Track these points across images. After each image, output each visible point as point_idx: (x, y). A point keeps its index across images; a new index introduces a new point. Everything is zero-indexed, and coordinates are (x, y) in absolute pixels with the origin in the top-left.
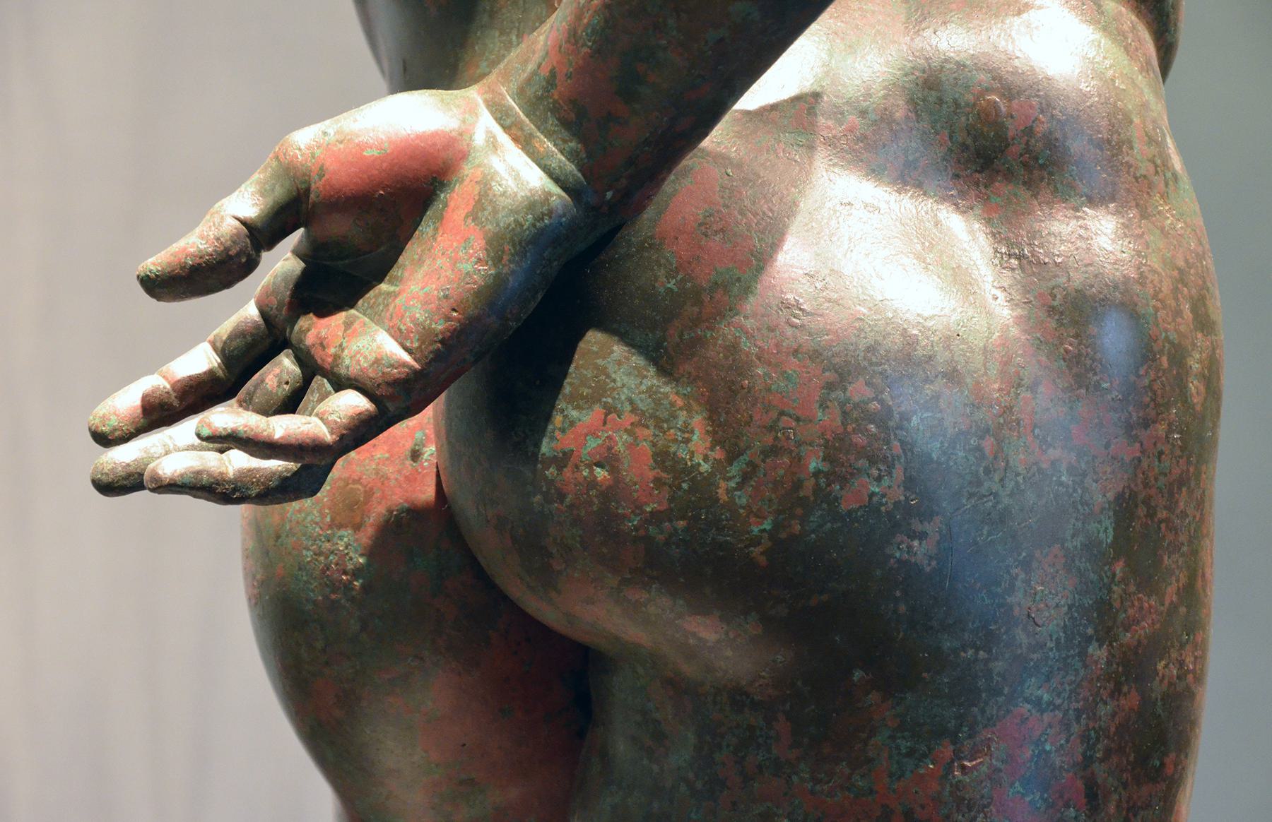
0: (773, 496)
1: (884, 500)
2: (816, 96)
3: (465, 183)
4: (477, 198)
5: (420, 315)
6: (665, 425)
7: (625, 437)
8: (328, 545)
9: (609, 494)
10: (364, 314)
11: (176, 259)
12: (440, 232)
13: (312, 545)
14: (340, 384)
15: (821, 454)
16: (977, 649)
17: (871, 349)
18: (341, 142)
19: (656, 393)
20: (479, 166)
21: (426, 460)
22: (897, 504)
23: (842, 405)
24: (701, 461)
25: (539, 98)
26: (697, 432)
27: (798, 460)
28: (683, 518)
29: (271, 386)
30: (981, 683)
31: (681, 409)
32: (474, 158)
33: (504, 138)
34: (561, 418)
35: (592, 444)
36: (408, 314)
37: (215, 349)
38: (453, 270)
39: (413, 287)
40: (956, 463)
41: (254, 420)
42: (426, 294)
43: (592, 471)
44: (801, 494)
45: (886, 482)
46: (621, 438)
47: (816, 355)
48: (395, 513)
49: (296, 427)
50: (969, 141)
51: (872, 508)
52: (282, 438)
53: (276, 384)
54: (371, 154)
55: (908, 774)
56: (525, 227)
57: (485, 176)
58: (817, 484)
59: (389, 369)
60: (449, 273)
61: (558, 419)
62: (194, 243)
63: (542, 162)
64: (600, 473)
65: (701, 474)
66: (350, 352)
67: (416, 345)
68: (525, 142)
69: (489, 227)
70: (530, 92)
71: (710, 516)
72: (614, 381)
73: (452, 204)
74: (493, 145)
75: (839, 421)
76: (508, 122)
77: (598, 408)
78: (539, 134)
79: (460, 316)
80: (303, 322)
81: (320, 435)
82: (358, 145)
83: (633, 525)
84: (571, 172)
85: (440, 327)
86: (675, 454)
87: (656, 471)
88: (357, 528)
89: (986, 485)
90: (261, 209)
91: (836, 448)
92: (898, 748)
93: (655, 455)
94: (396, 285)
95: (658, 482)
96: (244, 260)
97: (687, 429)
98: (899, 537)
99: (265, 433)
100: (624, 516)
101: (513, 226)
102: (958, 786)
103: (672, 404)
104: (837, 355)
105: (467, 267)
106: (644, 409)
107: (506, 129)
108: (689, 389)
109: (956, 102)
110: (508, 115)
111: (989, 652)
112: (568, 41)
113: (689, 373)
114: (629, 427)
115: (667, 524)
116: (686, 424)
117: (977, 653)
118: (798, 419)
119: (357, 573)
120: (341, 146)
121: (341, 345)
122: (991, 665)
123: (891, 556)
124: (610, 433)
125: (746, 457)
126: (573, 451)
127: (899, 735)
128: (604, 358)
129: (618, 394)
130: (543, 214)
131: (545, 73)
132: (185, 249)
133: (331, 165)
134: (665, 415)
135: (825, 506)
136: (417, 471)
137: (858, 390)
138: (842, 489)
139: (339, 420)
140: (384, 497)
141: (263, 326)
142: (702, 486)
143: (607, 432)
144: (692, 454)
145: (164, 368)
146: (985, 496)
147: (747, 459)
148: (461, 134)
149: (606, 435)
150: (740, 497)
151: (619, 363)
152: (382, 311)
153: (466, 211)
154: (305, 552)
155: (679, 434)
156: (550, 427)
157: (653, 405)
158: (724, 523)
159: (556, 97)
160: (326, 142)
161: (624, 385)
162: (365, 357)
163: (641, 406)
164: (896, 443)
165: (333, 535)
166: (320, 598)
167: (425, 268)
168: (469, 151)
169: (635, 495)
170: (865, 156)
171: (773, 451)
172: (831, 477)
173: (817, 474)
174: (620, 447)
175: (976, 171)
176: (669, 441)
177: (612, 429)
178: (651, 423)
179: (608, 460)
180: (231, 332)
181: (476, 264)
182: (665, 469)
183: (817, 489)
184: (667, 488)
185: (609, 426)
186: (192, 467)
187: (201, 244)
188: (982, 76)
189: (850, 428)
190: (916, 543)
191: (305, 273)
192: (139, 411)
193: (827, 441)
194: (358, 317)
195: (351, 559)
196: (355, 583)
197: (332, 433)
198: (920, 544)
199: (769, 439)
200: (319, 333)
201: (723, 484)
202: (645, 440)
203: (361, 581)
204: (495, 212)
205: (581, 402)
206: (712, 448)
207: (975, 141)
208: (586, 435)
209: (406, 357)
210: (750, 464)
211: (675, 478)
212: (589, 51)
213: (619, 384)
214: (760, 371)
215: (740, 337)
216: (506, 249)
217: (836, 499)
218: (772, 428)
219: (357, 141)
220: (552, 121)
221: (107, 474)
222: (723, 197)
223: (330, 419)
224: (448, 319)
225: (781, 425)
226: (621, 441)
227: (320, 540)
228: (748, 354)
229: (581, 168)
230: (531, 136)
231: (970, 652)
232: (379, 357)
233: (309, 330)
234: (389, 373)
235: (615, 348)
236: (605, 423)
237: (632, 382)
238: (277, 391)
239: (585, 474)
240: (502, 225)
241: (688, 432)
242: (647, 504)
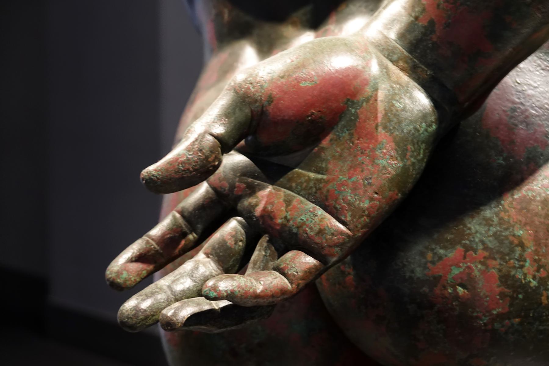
6: (507, 258)
7: (479, 266)
9: (464, 303)
10: (299, 194)
19: (500, 236)
24: (531, 280)
26: (528, 261)
28: (517, 317)
29: (230, 243)
34: (431, 255)
35: (456, 271)
41: (243, 282)
43: (455, 290)
46: (476, 266)
52: (262, 291)
53: (233, 243)
54: (305, 85)
56: (421, 132)
65: (531, 288)
71: (536, 314)
72: (470, 229)
76: (395, 57)
77: (459, 247)
78: (420, 65)
81: (285, 286)
82: (296, 79)
85: (366, 205)
86: (514, 276)
93: (501, 277)
95: (503, 295)
97: (522, 259)
100: (478, 318)
101: (413, 132)
103: (511, 243)
106: (492, 247)
113: (520, 221)
114: (482, 260)
115: (507, 321)
116: (521, 256)
120: (283, 80)
124: (469, 264)
126: (441, 276)
129: (473, 238)
134: (507, 251)
139: (296, 274)
144: (525, 275)
145: (148, 233)
149: (465, 265)
155: (516, 262)
157: (498, 244)
158: (544, 318)
162: (311, 228)
163: (490, 245)
174: (476, 273)
176: (510, 268)
177: (470, 262)
182: (508, 287)
184: (508, 298)
185: (468, 259)
187: (190, 155)
194: (294, 197)
202: (494, 268)
205: (446, 244)
208: (451, 266)
211: (514, 292)
213: (473, 231)
216: (409, 148)
224: (372, 199)
226: (477, 269)
232: (322, 228)
234: (331, 239)
236: (465, 257)
237: (482, 229)
238: (235, 247)
240: (405, 131)
241: (522, 261)
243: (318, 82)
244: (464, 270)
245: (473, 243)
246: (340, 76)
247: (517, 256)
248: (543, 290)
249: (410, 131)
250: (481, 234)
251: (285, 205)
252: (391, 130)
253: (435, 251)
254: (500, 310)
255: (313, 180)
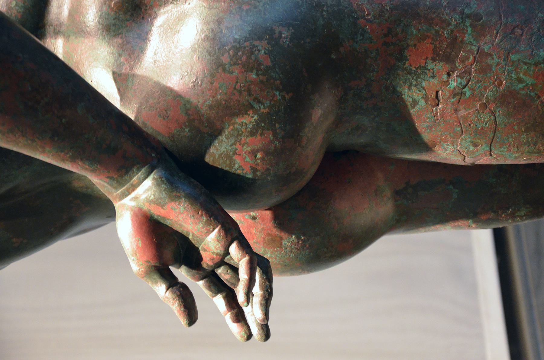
0: (266, 91)
1: (267, 48)
2: (114, 73)
3: (150, 209)
4: (156, 205)
5: (200, 226)
7: (245, 147)
8: (288, 249)
9: (266, 152)
10: (201, 244)
11: (182, 314)
12: (169, 218)
13: (288, 254)
14: (227, 253)
15: (250, 73)
16: (323, 11)
17: (210, 54)
18: (136, 255)
19: (228, 136)
20: (144, 204)
21: (256, 214)
22: (268, 43)
23: (231, 65)
24: (254, 119)
25: (117, 182)
26: (242, 121)
27: (252, 82)
28: (275, 125)
30: (336, 8)
31: (234, 127)
32: (141, 205)
33: (133, 195)
35: (248, 159)
36: (200, 230)
37: (215, 296)
38: (183, 214)
39: (190, 228)
40: (253, 20)
42: (193, 223)
43: (258, 159)
44: (265, 80)
45: (260, 48)
46: (245, 149)
47: (212, 76)
48: (276, 225)
49: (243, 271)
50: (129, 13)
51: (269, 53)
52: (247, 276)
53: (228, 275)
55: (370, 36)
56: (166, 187)
57: (147, 202)
58: (261, 74)
59: (221, 237)
60: (184, 215)
61: (239, 172)
62: (176, 308)
63: (142, 180)
64: (259, 156)
65: (258, 119)
66: (215, 250)
67: (212, 227)
68: (134, 187)
69: (167, 200)
70: (115, 185)
71: (274, 115)
72: (224, 151)
73: (158, 214)
74: (135, 199)
75: (238, 67)
76: (127, 193)
77: (234, 157)
78: (131, 182)
79: (201, 211)
80: (205, 266)
81: (246, 261)
82: (137, 249)
83: (278, 143)
84: (145, 170)
86: (251, 129)
87: (257, 135)
88: (281, 238)
89: (260, 8)
90: (162, 283)
91: (248, 68)
92: (361, 40)
93: (252, 136)
94: (190, 233)
95: (262, 135)
96: (181, 289)
97: (241, 124)
98: (281, 42)
99: (246, 282)
100: (275, 147)
102: (375, 17)
103: (232, 130)
104: (212, 68)
105: (182, 209)
107: (129, 194)
108: (226, 124)
109: (115, 19)
110: (124, 193)
111: (324, 6)
112: (96, 173)
113: (220, 124)
114: (241, 146)
115: (277, 131)
116: (240, 125)
117: (324, 11)
118: (237, 82)
119: (298, 238)
121: (213, 253)
122: (329, 5)
123: (288, 46)
124: (243, 153)
125: (252, 102)
126: (251, 167)
127: (356, 40)
128: (216, 155)
129: (229, 150)
130: (161, 180)
131: (108, 180)
132: (178, 311)
133: (145, 258)
134: (236, 133)
135: (269, 71)
136: (260, 218)
137: (226, 59)
138: (263, 65)
139: (241, 254)
140: (270, 230)
141: (206, 279)
142: (263, 118)
143: (243, 154)
144: (251, 122)
145: (223, 314)
146: (265, 9)
147: (252, 101)
148: (132, 210)
150: (267, 104)
151: (217, 150)
152: (199, 238)
153: (161, 209)
154: (291, 256)
155: (243, 127)
156: (242, 174)
157: (233, 137)
158: (277, 109)
159: (117, 176)
160: (137, 260)
161: (226, 148)
162: (217, 245)
163: (233, 141)
164: (246, 44)
165: (284, 247)
166: (308, 250)
167: (183, 223)
168: (138, 208)
169: (267, 143)
170: (136, 54)
171: (249, 91)
172: (258, 69)
173: (257, 75)
174: (249, 149)
175: (141, 10)
176: (246, 131)
177: (242, 152)
178: (239, 138)
179: (254, 153)
180: (209, 291)
181: (181, 205)
182: (257, 132)
183: (263, 74)
184: (264, 131)
186: (259, 307)
188: (104, 9)
189: (240, 62)
190: (283, 36)
191: (186, 265)
192: (239, 324)
193: (245, 71)
194: (202, 246)
195: (293, 240)
196: (302, 238)
197: (245, 257)
198: (283, 34)
199: (245, 93)
200: (208, 260)
201: (262, 111)
202: (246, 140)
203: (301, 237)
204: (161, 198)
206: (249, 115)
207: (129, 11)
208: (244, 161)
209: (216, 230)
210: (254, 100)
211: (260, 128)
212: (99, 165)
213: (225, 150)
214: (219, 97)
215: (206, 105)
216: (175, 194)
217: (267, 67)
218: (240, 92)
219: (136, 249)
220: (126, 177)
221: (262, 337)
222: (153, 110)
223: (240, 258)
224: (202, 215)
225: (239, 89)
226: (246, 149)
227: (286, 251)
228: (212, 102)
229: (143, 166)
230: (132, 185)
231: (324, 13)
233: (207, 264)
234: (222, 237)
235: (211, 151)
236: (240, 155)
237: (224, 145)
238: (230, 274)
239: (259, 162)
240: (166, 196)
241: (242, 124)
242: (270, 138)
243: (139, 237)
244: (246, 155)
245: (232, 151)
246: (136, 225)
247: (239, 127)
248: (260, 111)
249: (166, 193)
250: (227, 146)
251: (206, 252)
252: (165, 203)
253: (236, 169)
254: (270, 135)
255: (193, 238)
